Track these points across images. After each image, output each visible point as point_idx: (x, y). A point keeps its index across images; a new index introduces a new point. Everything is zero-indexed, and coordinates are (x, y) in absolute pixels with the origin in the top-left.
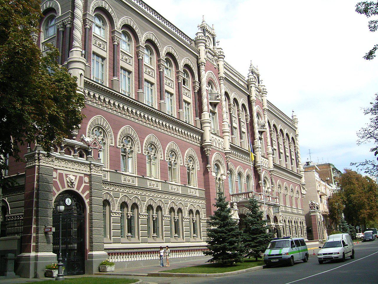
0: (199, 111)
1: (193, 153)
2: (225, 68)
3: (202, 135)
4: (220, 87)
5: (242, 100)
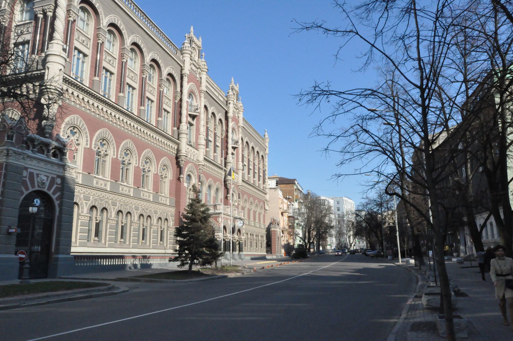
0: (177, 122)
2: (207, 81)
3: (178, 144)
4: (200, 99)
5: (220, 116)
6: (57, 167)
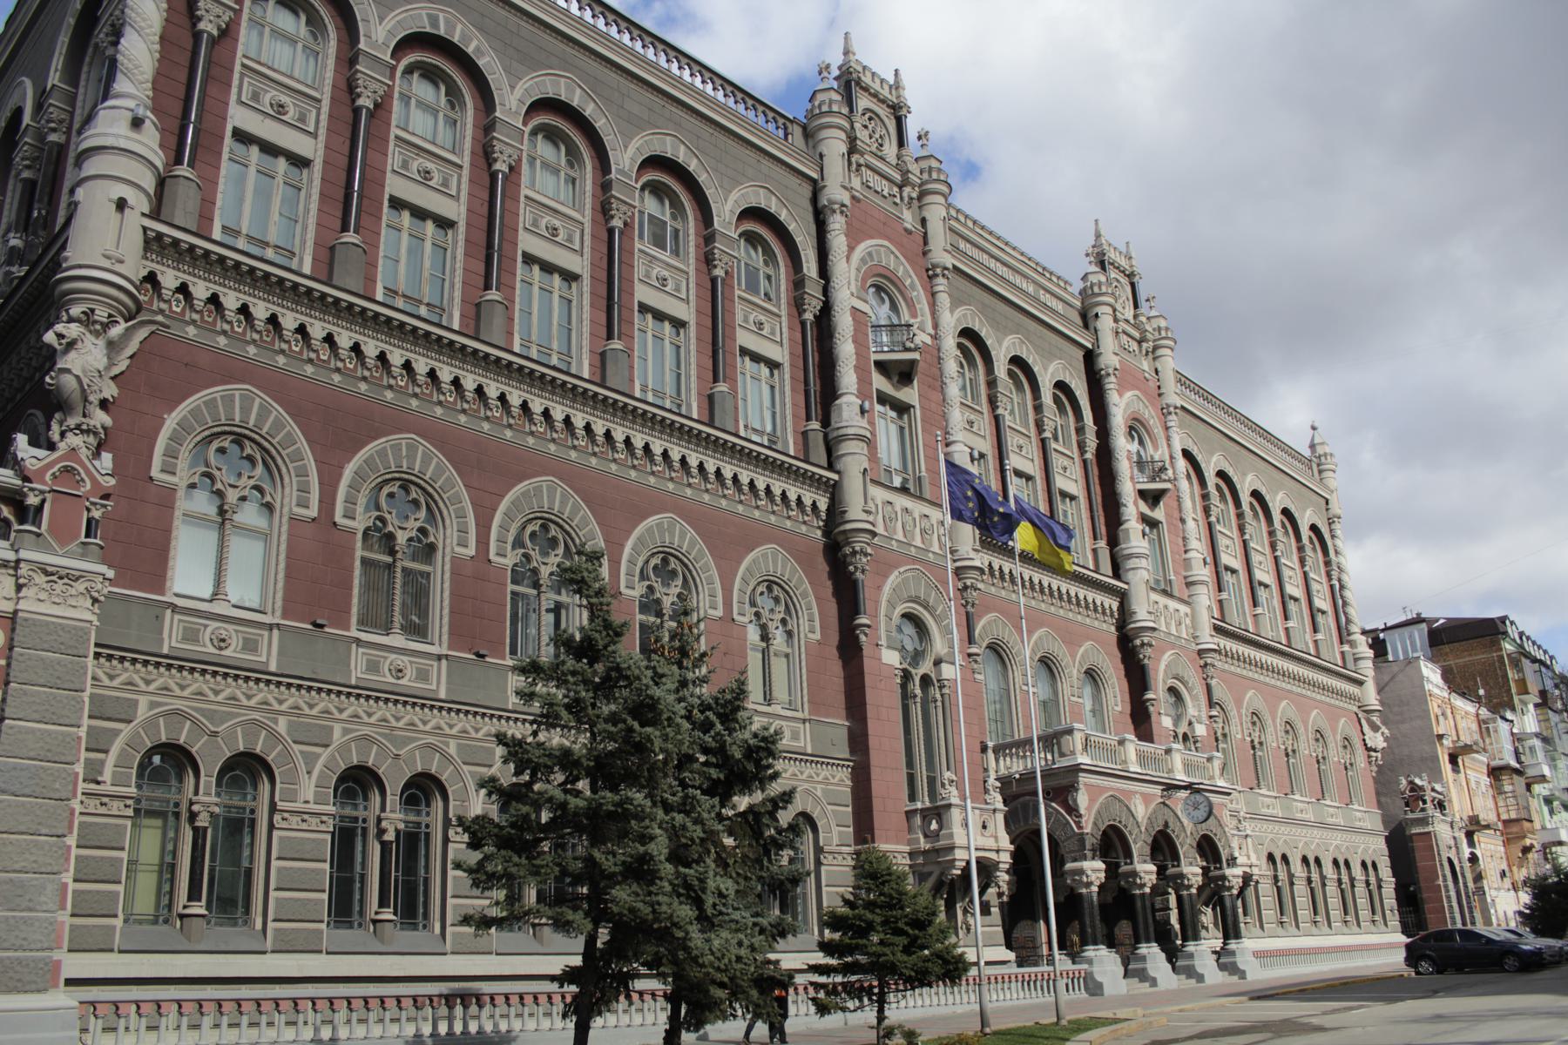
3: (835, 491)
4: (933, 305)
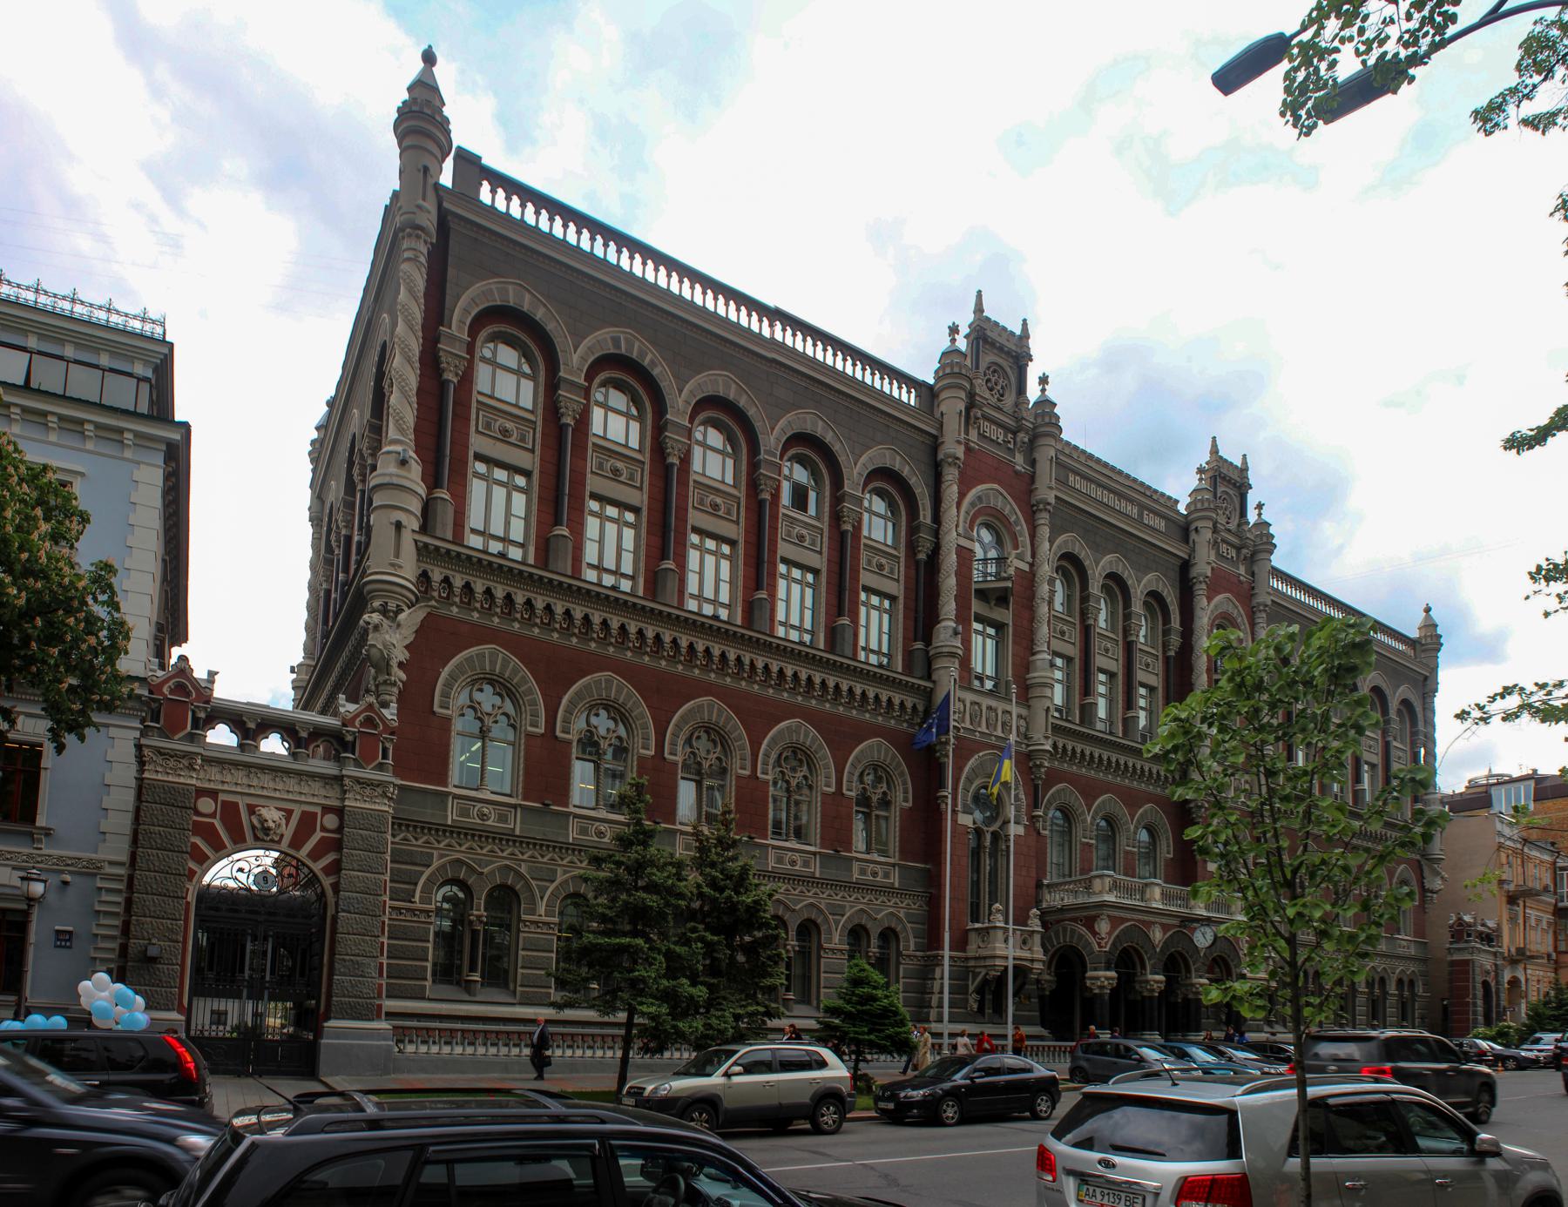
1: (886, 755)
4: (1033, 536)
6: (321, 784)
